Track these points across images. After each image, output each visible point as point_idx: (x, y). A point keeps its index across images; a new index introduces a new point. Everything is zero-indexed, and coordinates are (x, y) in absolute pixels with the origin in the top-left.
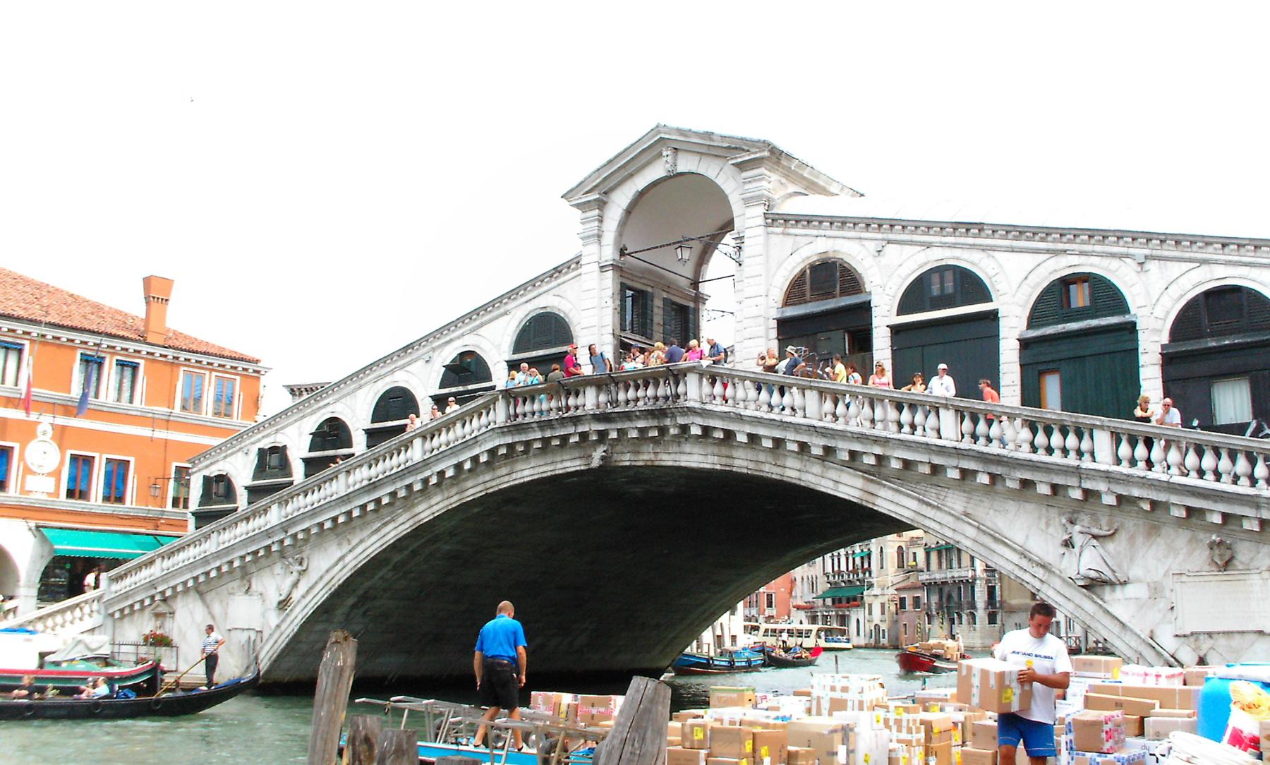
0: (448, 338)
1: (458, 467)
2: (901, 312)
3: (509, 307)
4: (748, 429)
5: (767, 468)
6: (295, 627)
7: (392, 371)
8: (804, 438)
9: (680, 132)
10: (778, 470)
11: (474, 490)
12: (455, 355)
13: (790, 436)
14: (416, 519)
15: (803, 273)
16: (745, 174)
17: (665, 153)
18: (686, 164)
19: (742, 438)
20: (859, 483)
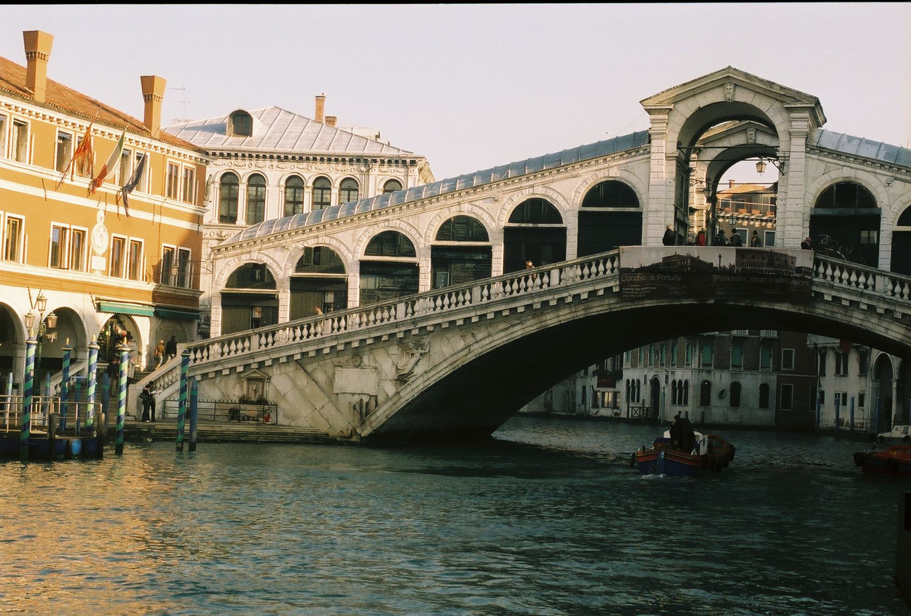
0: (519, 186)
2: (899, 224)
4: (834, 293)
5: (839, 316)
6: (415, 393)
8: (875, 304)
9: (747, 75)
10: (847, 319)
11: (597, 308)
13: (864, 301)
14: (543, 324)
15: (830, 188)
16: (793, 115)
18: (742, 96)
19: (828, 298)
20: (902, 331)
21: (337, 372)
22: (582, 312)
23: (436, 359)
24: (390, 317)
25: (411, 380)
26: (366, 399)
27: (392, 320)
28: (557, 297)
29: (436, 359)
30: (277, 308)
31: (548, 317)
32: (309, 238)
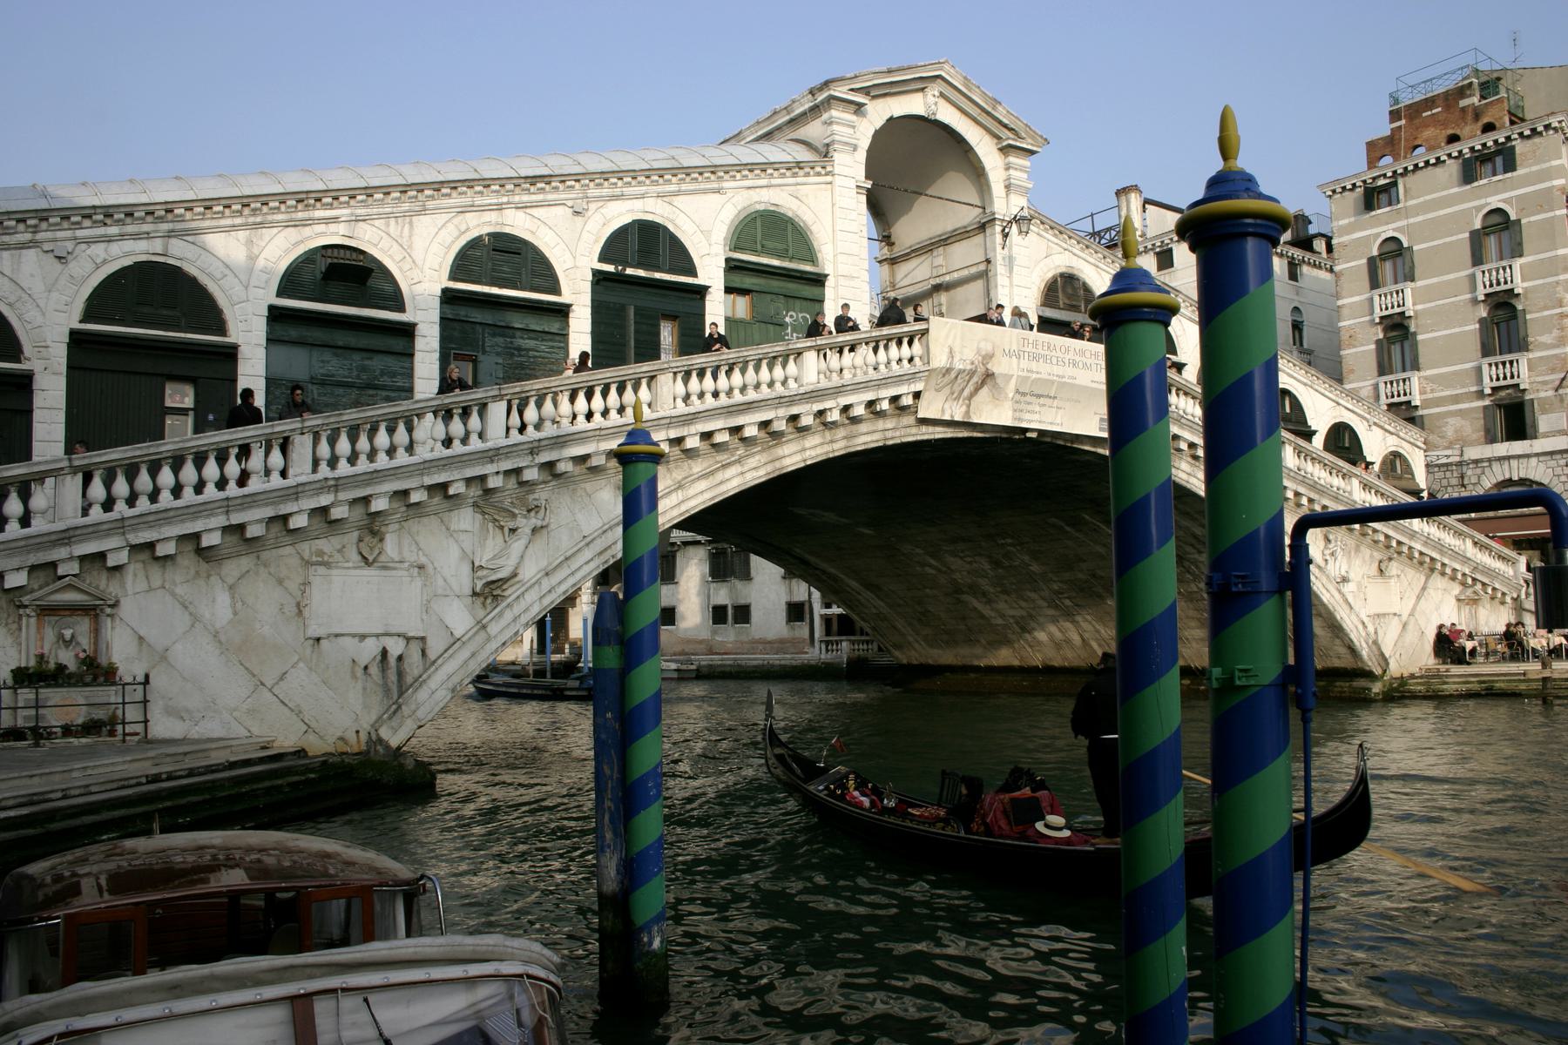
0: (617, 191)
1: (870, 404)
3: (726, 185)
7: (500, 208)
12: (627, 220)
14: (778, 465)
16: (1012, 159)
17: (934, 90)
18: (948, 115)
21: (316, 582)
22: (841, 444)
23: (563, 541)
24: (467, 434)
25: (511, 592)
26: (395, 647)
27: (475, 444)
28: (817, 407)
29: (563, 541)
30: (31, 411)
31: (786, 449)
32: (122, 237)
